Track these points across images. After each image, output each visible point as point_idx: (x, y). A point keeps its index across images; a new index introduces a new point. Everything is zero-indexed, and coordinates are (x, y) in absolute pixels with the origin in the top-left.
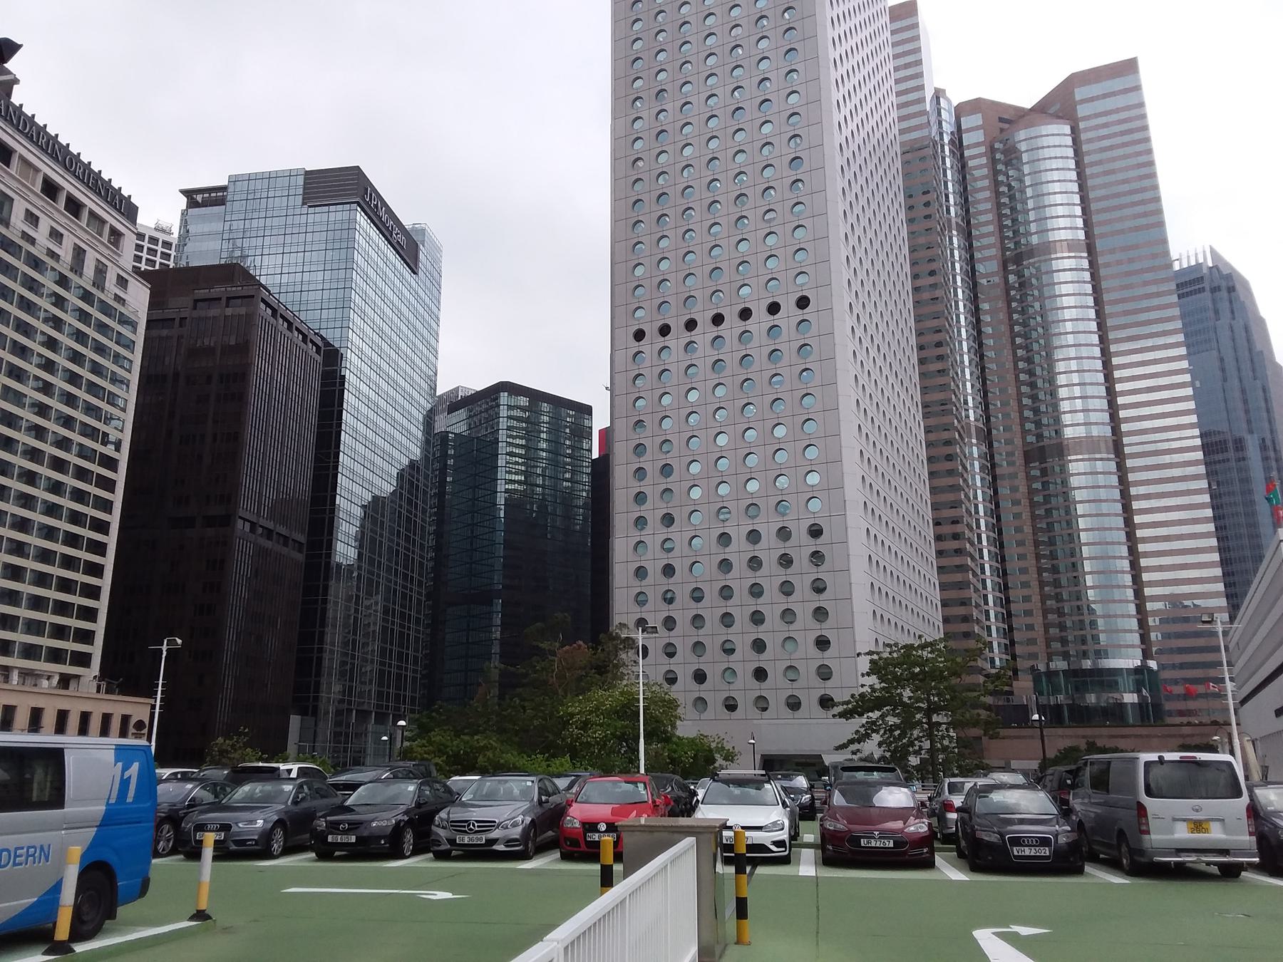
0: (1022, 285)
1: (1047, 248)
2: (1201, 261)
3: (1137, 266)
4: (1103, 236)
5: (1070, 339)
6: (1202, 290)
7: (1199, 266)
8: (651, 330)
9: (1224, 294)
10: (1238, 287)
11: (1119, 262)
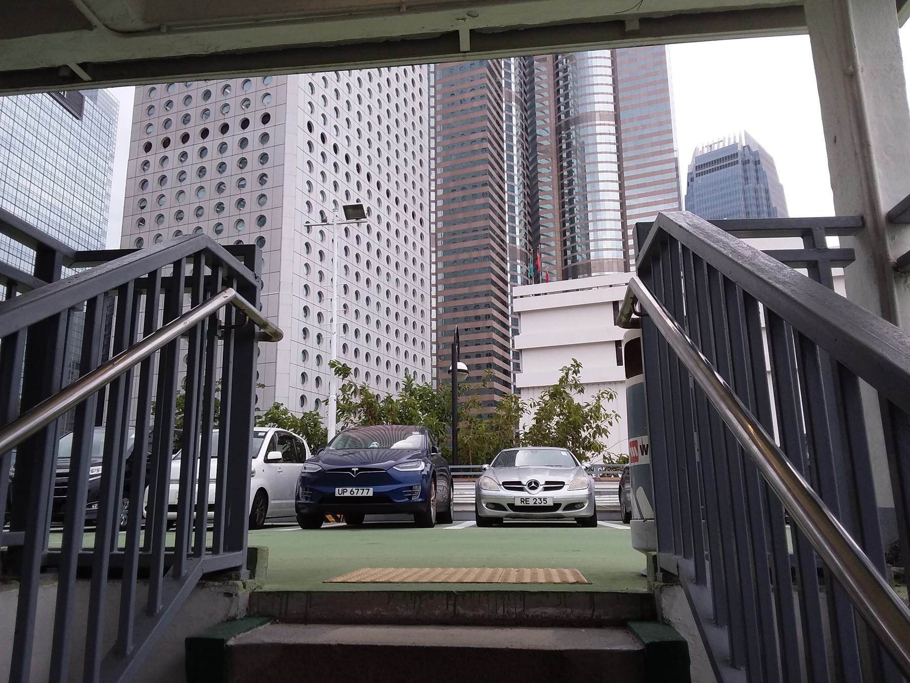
1: (590, 116)
2: (737, 141)
3: (647, 131)
4: (626, 108)
8: (157, 143)
9: (752, 165)
10: (762, 160)
11: (636, 129)
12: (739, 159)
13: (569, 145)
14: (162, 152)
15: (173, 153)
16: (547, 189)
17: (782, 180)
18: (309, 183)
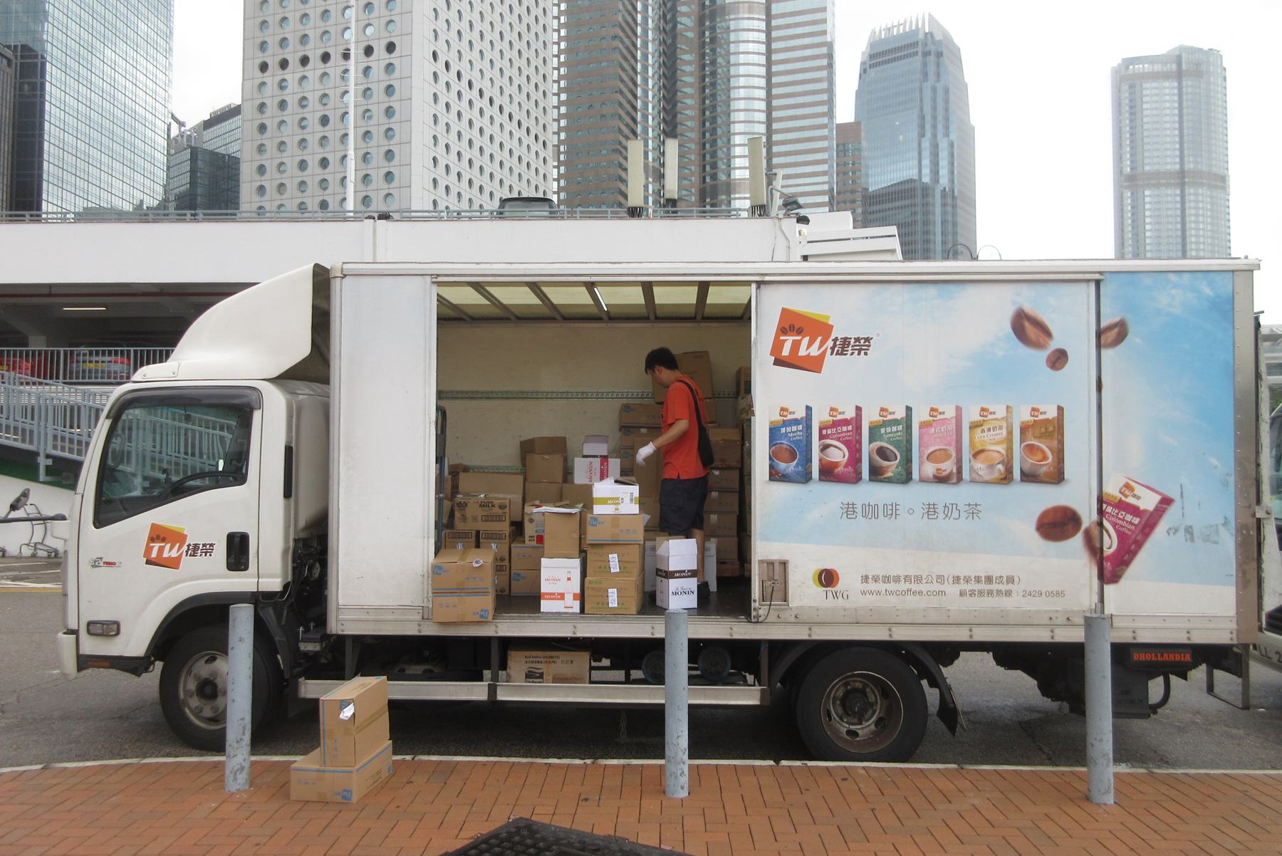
0: (713, 40)
5: (742, 93)
6: (916, 54)
7: (916, 32)
8: (273, 63)
10: (945, 51)
12: (920, 49)
13: (713, 40)
14: (280, 74)
15: (292, 76)
16: (688, 90)
17: (968, 77)
18: (435, 116)
